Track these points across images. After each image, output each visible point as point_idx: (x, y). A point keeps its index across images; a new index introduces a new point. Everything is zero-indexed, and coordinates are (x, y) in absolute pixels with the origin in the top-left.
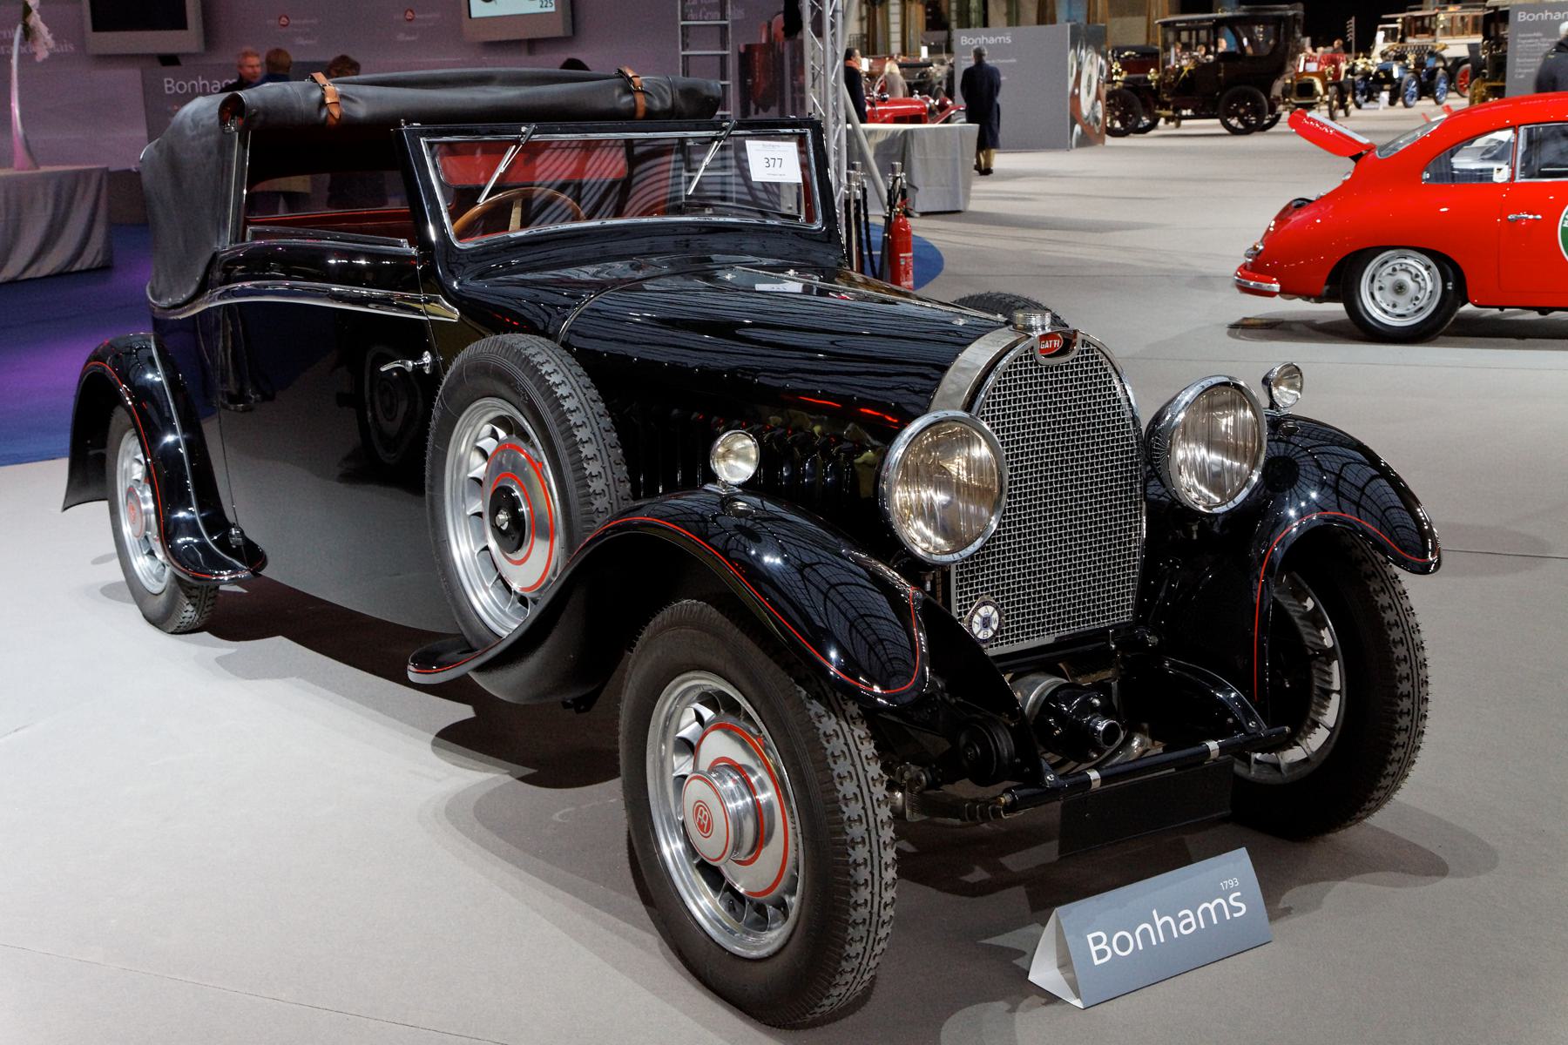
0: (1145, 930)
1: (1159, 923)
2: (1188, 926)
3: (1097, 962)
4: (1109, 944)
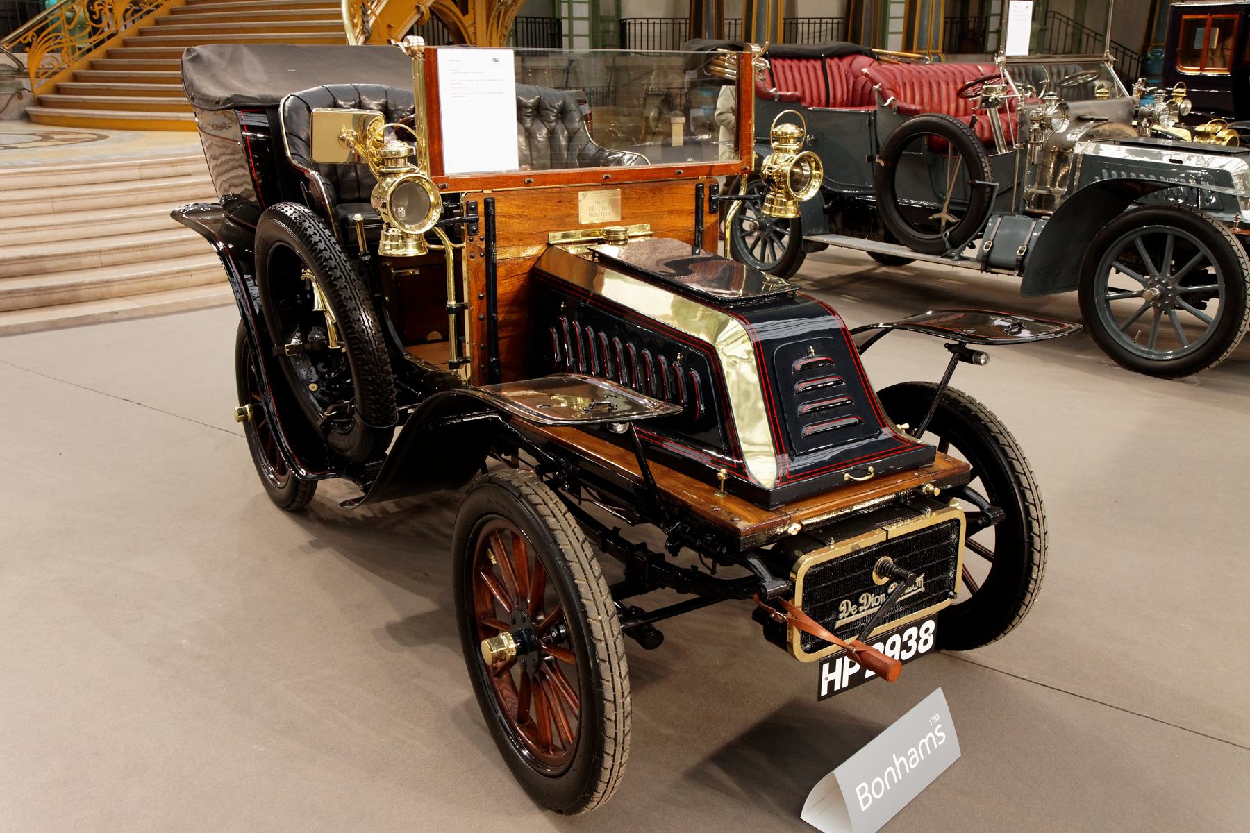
0: (890, 773)
1: (897, 764)
2: (914, 762)
3: (864, 809)
4: (870, 792)
